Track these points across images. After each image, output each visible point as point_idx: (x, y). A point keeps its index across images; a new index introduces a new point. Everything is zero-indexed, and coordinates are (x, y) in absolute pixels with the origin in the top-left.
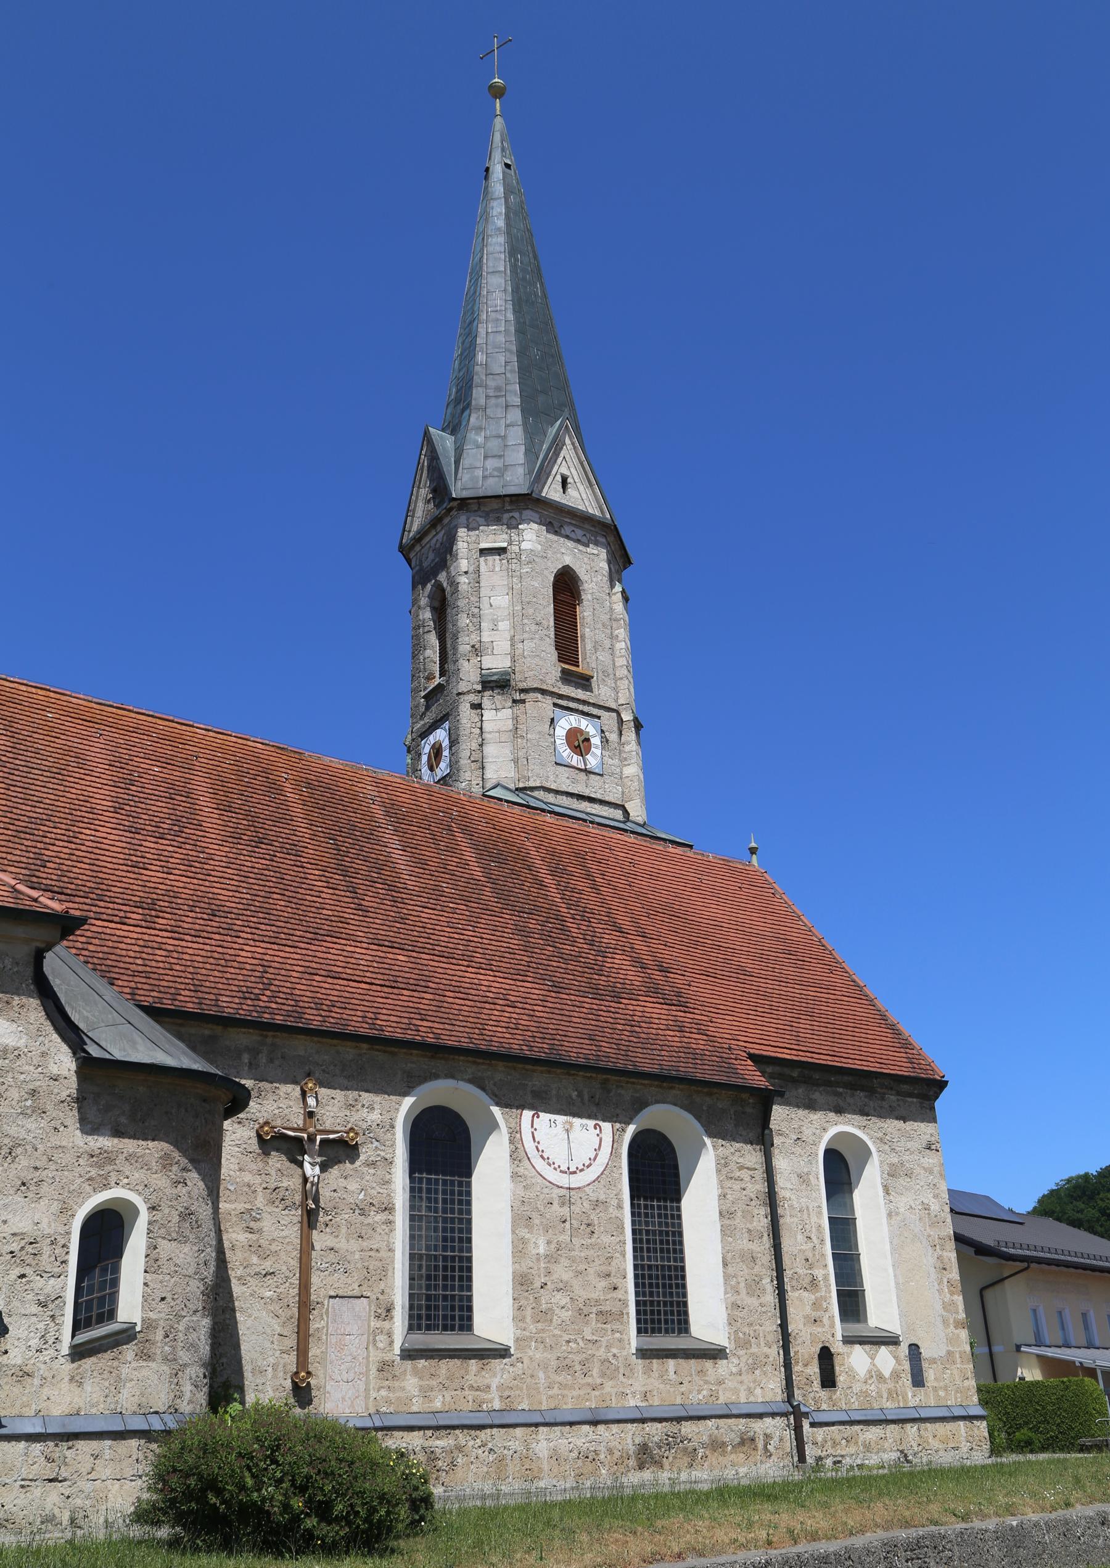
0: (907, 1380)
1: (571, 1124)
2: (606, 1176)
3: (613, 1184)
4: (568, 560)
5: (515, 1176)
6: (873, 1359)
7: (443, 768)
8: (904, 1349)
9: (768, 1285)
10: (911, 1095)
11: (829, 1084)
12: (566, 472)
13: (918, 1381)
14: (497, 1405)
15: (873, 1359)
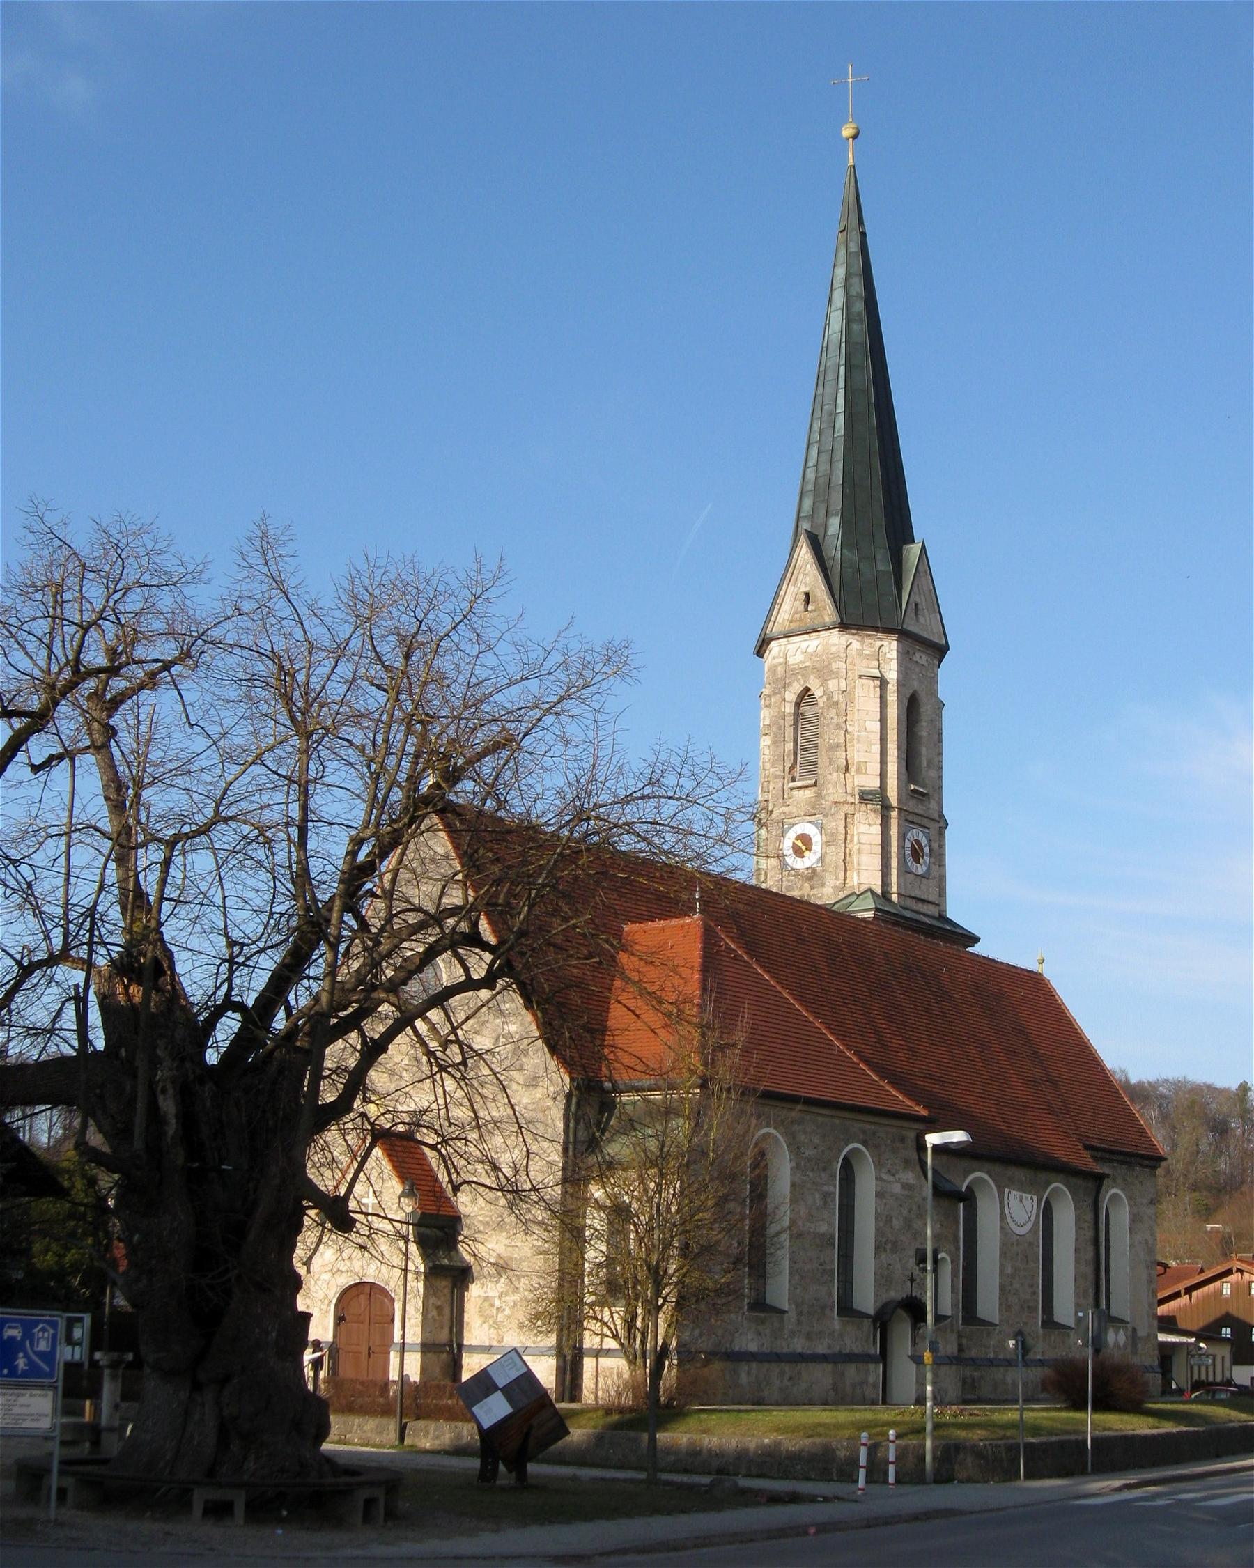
0: (1129, 1349)
1: (1021, 1197)
2: (1034, 1230)
3: (1036, 1233)
4: (916, 685)
5: (1002, 1228)
6: (1116, 1334)
7: (810, 859)
8: (1130, 1333)
9: (1091, 1292)
10: (1146, 1166)
11: (1111, 1161)
12: (918, 600)
13: (1135, 1352)
14: (992, 1355)
15: (1116, 1334)
